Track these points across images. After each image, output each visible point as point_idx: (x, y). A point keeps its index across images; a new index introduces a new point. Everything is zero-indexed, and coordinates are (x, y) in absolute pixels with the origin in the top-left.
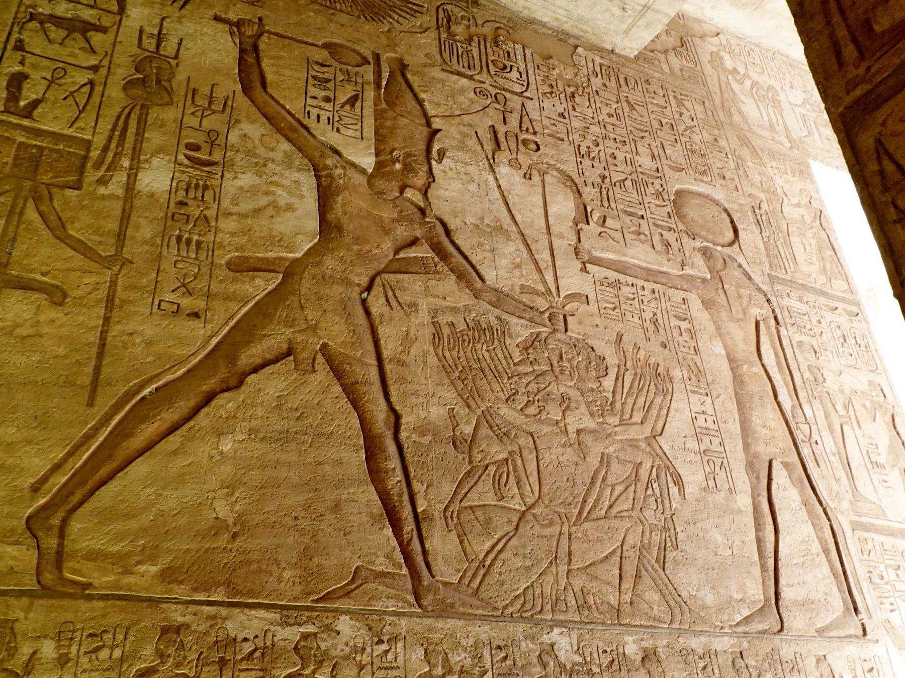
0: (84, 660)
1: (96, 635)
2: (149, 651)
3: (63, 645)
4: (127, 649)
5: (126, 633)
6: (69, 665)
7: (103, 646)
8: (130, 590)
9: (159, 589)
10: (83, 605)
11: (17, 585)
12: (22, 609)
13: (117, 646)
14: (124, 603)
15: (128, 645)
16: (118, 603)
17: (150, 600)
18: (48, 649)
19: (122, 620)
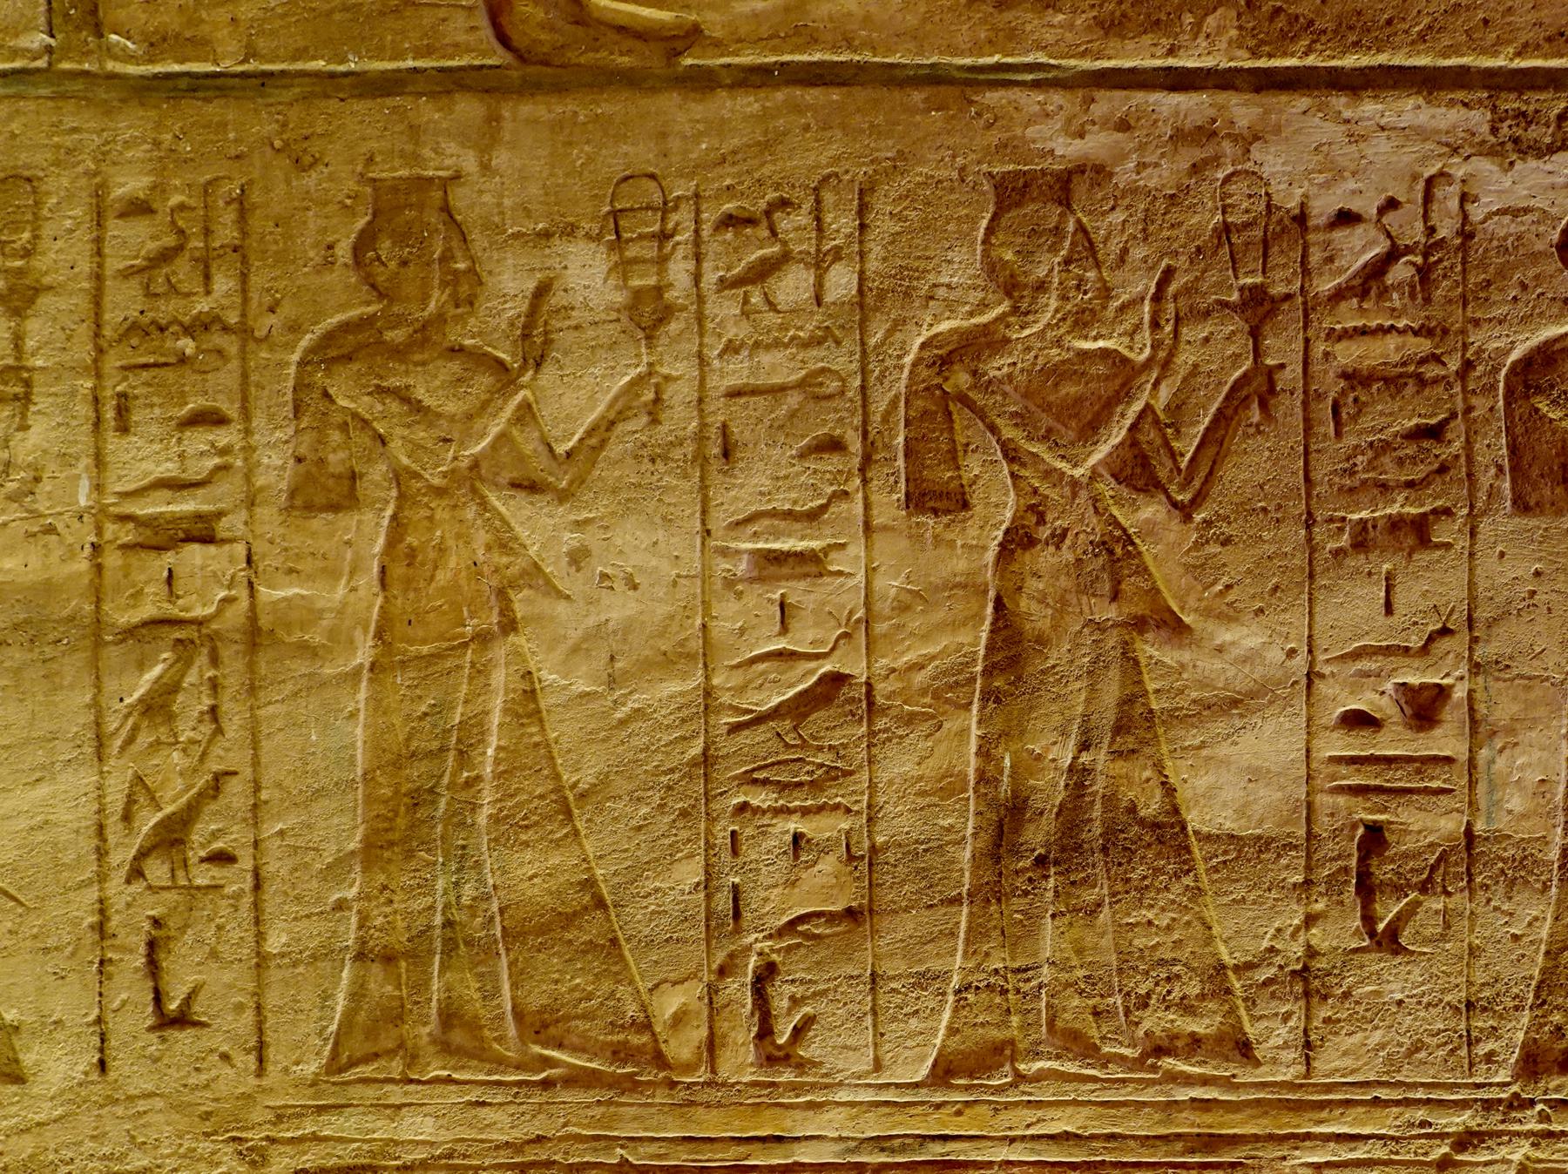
0: (723, 309)
1: (751, 221)
2: (959, 269)
3: (635, 261)
4: (873, 265)
5: (863, 209)
6: (674, 327)
7: (785, 258)
8: (849, 43)
9: (963, 36)
10: (680, 112)
11: (428, 52)
12: (464, 139)
13: (837, 253)
14: (835, 95)
15: (876, 250)
16: (812, 95)
17: (934, 78)
18: (587, 275)
19: (836, 160)
